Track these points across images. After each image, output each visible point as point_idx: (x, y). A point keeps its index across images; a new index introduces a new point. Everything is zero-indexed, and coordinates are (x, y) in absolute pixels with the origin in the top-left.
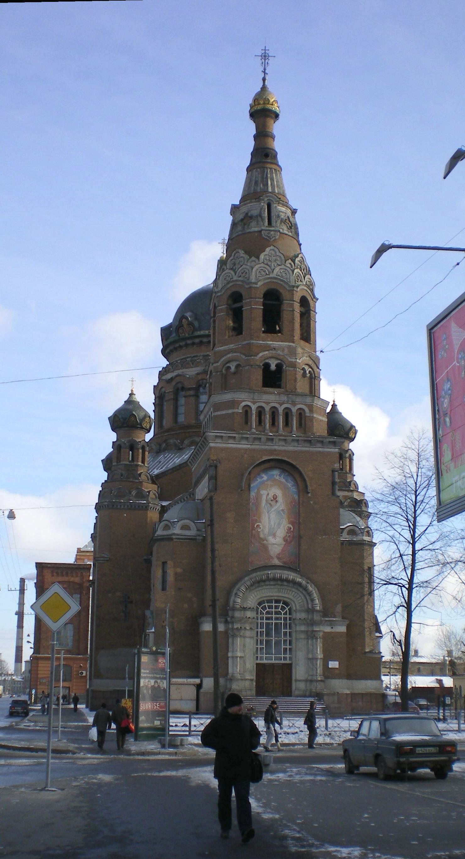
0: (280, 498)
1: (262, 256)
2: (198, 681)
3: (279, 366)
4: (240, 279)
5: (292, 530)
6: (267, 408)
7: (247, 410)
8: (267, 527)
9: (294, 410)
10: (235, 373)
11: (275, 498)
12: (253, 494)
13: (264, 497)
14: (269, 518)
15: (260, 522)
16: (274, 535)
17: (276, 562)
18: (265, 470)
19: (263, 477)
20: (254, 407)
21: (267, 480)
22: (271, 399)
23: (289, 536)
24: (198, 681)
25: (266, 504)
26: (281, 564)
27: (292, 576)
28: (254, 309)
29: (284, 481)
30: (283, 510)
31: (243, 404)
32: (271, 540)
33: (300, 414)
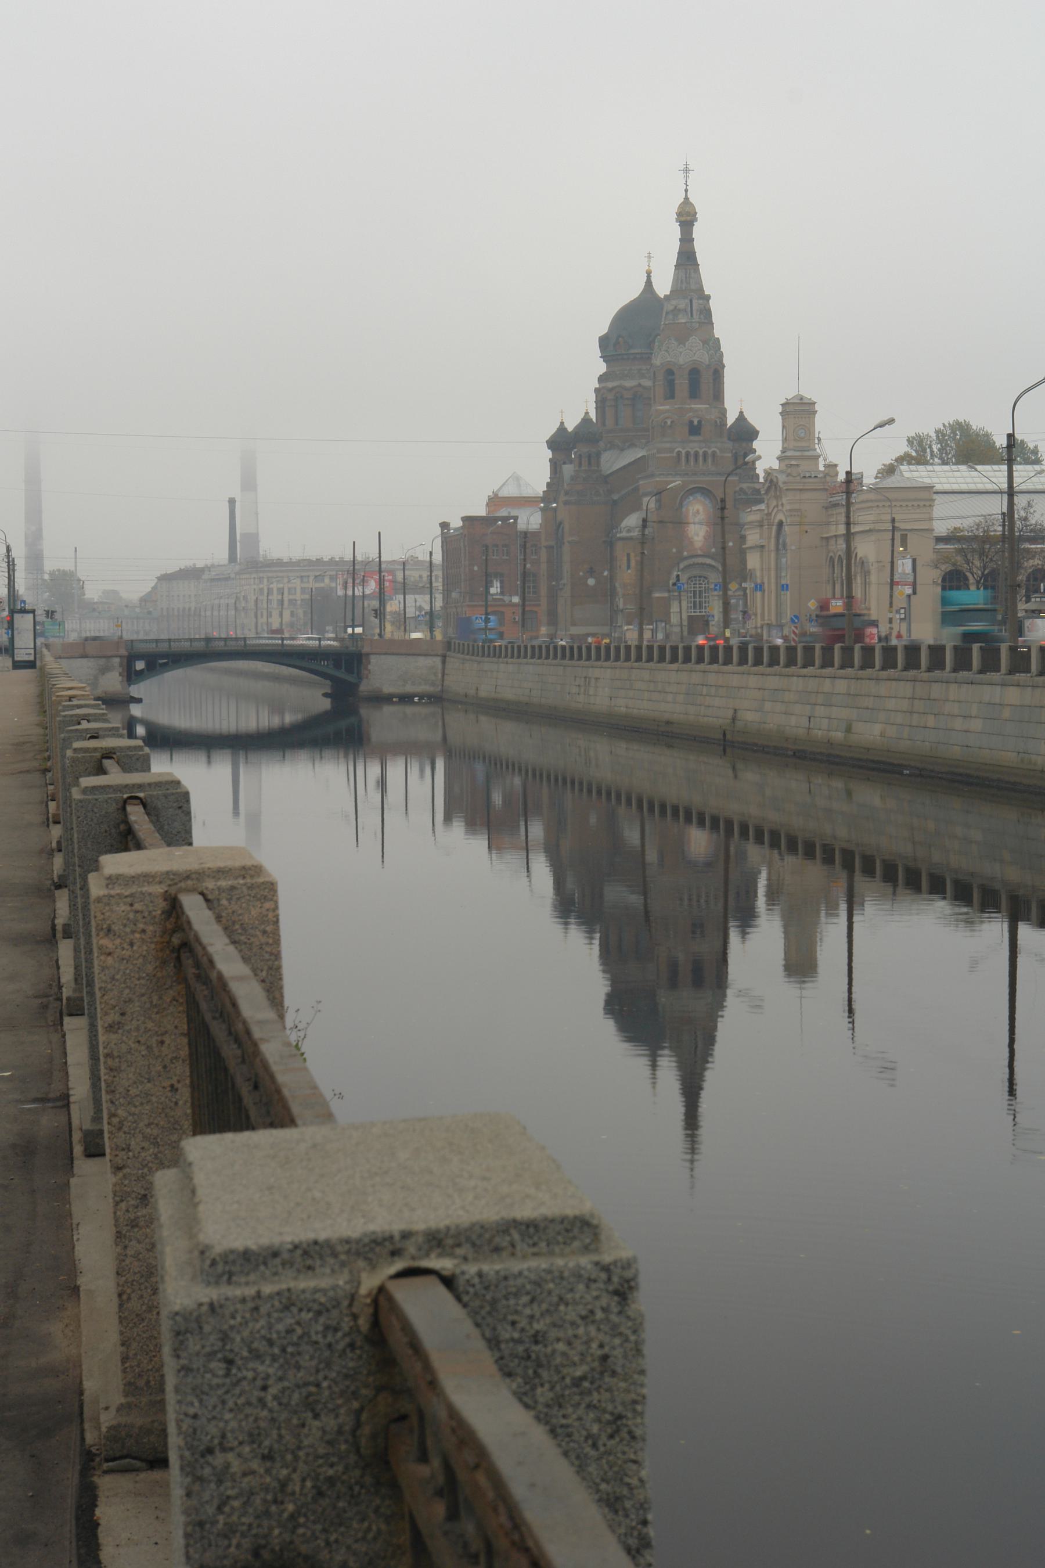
3: (699, 422)
6: (692, 452)
7: (679, 453)
9: (710, 452)
11: (698, 512)
12: (684, 510)
16: (698, 535)
17: (699, 552)
18: (691, 494)
20: (683, 452)
22: (695, 446)
27: (708, 561)
28: (682, 383)
32: (696, 538)
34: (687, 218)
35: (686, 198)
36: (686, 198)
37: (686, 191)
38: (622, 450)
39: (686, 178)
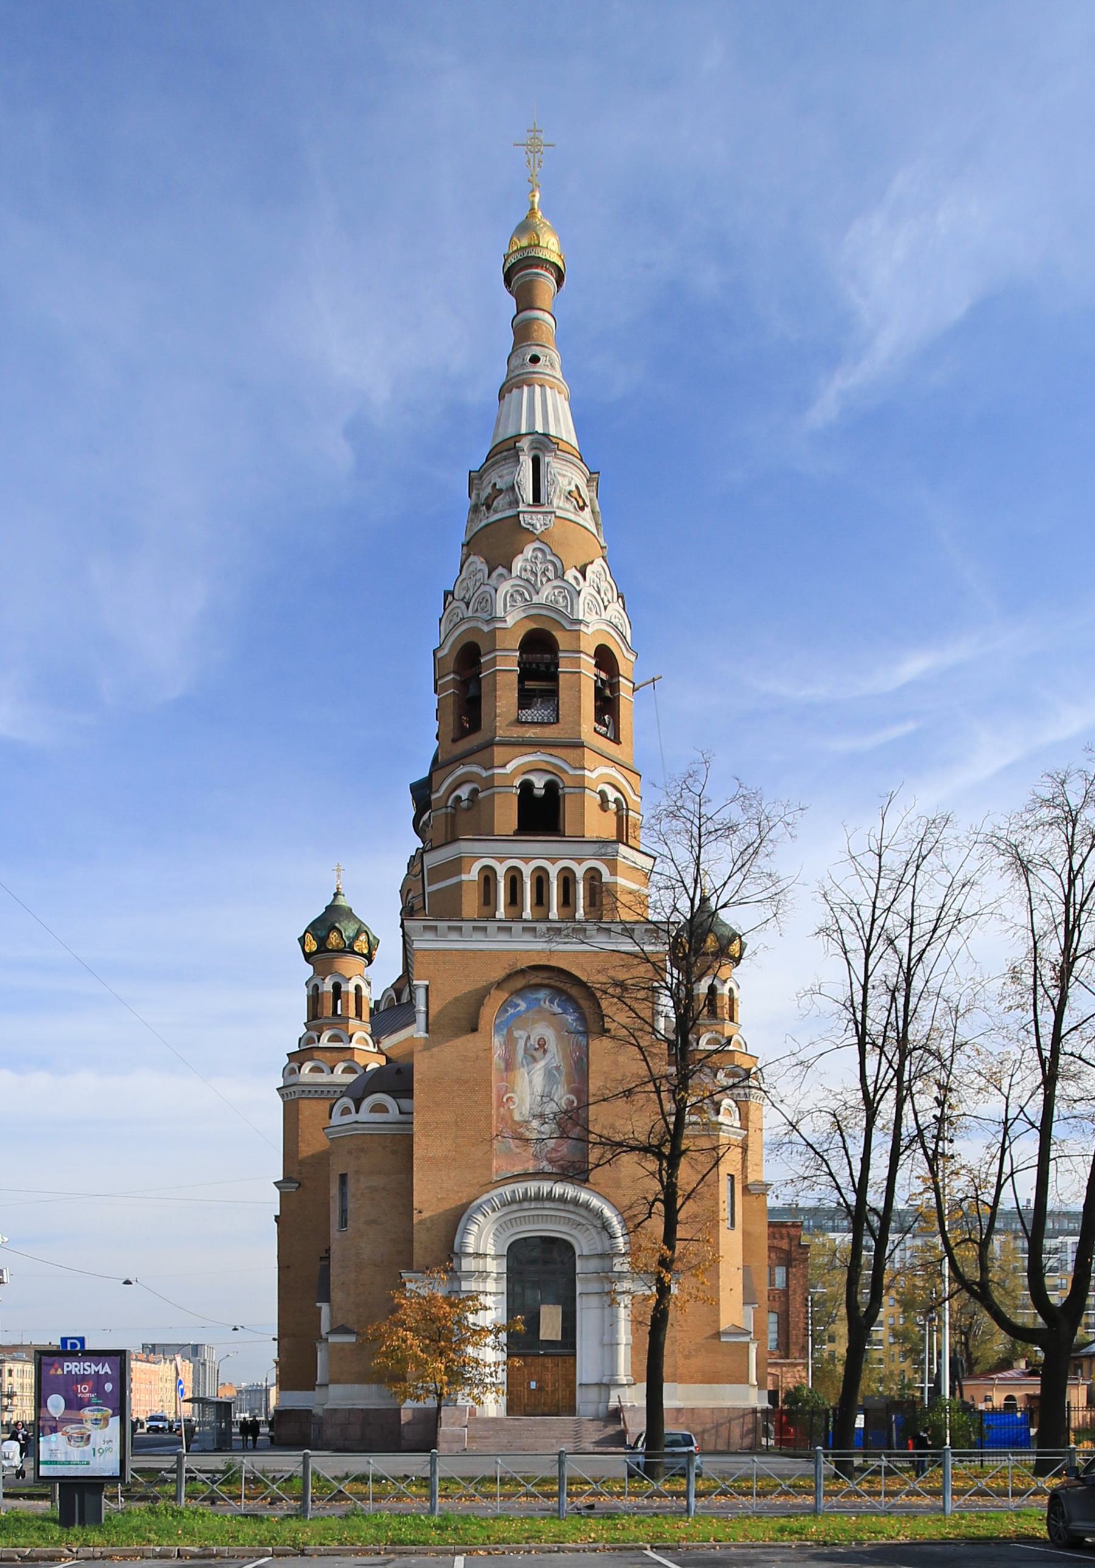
0: (552, 1045)
1: (518, 564)
3: (551, 787)
11: (542, 1045)
13: (521, 1044)
14: (531, 1082)
15: (513, 1092)
19: (518, 1005)
21: (528, 1009)
25: (525, 1057)
30: (557, 1068)
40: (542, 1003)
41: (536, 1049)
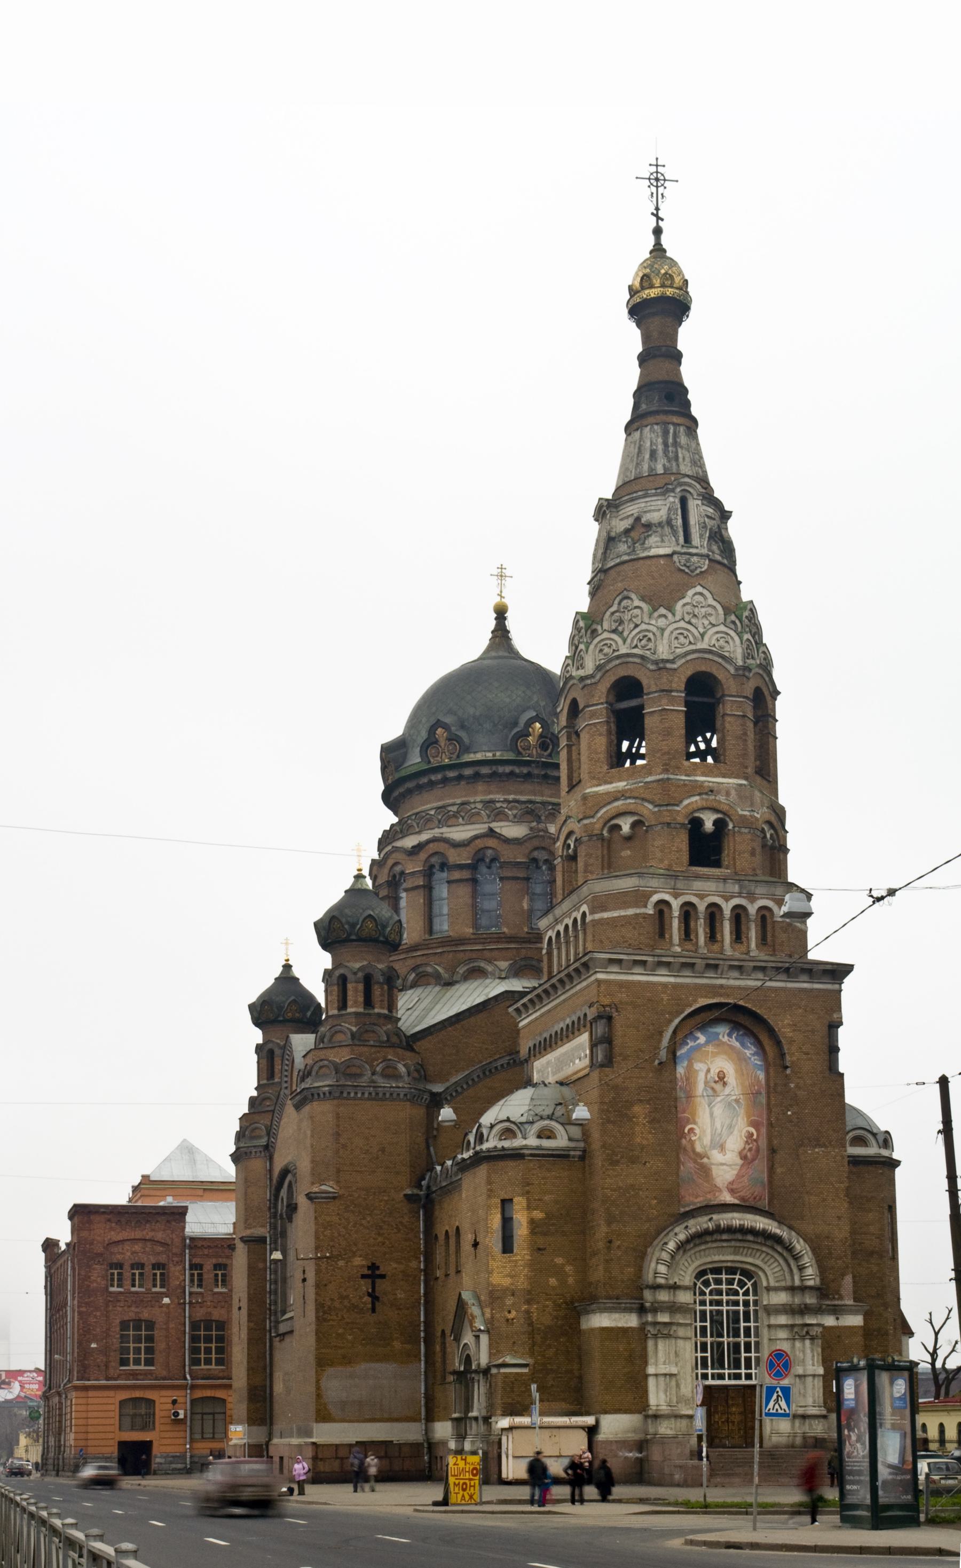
0: (731, 1078)
1: (679, 606)
2: (590, 1420)
3: (720, 824)
4: (635, 651)
5: (755, 1137)
6: (702, 907)
8: (708, 1131)
9: (752, 909)
10: (629, 838)
11: (721, 1078)
12: (681, 1070)
13: (701, 1076)
14: (712, 1114)
15: (695, 1123)
16: (722, 1148)
17: (728, 1198)
18: (703, 1027)
19: (698, 1038)
20: (676, 904)
21: (707, 1043)
22: (707, 890)
23: (750, 1150)
24: (590, 1420)
25: (705, 1089)
26: (737, 1202)
27: (761, 1223)
28: (665, 711)
29: (737, 1044)
30: (737, 1101)
31: (655, 898)
33: (763, 918)
34: (659, 307)
35: (658, 250)
36: (658, 250)
37: (658, 232)
38: (449, 984)
39: (657, 198)
40: (721, 1037)
41: (715, 1082)
